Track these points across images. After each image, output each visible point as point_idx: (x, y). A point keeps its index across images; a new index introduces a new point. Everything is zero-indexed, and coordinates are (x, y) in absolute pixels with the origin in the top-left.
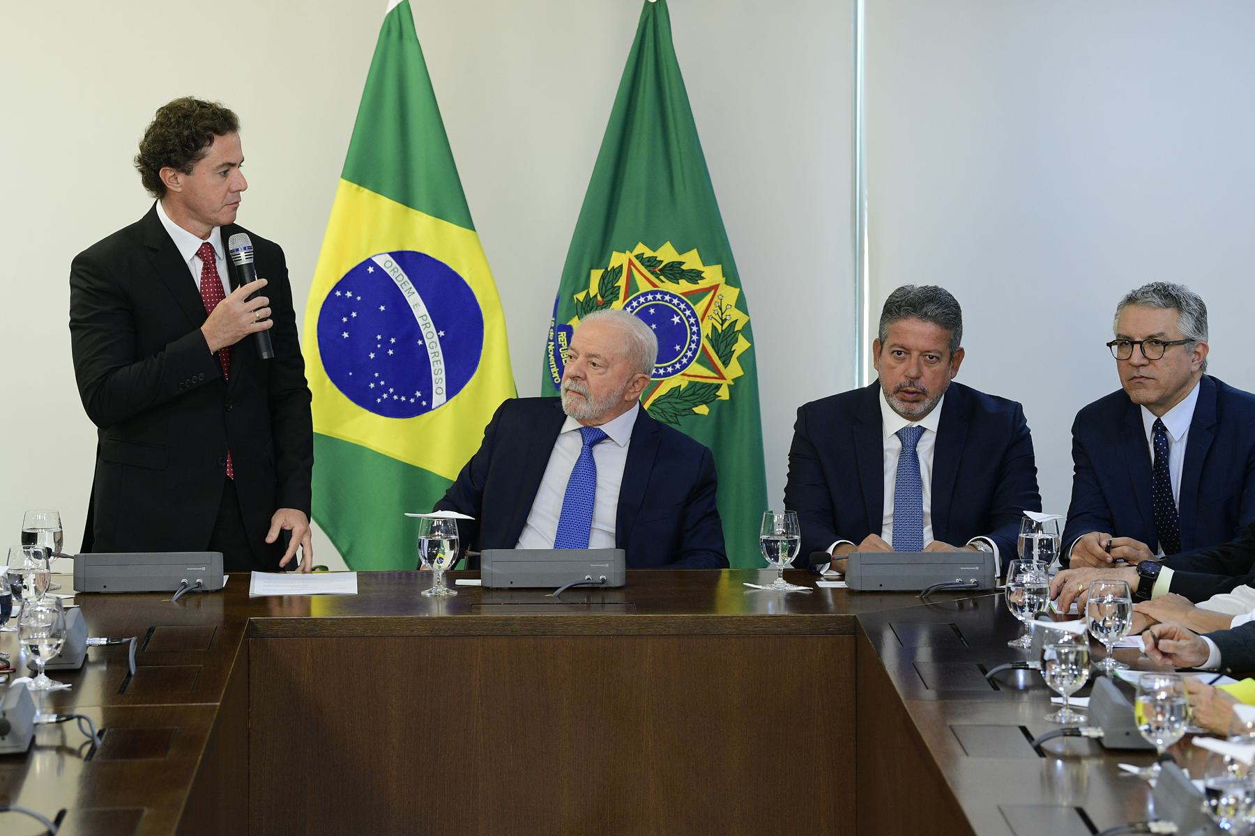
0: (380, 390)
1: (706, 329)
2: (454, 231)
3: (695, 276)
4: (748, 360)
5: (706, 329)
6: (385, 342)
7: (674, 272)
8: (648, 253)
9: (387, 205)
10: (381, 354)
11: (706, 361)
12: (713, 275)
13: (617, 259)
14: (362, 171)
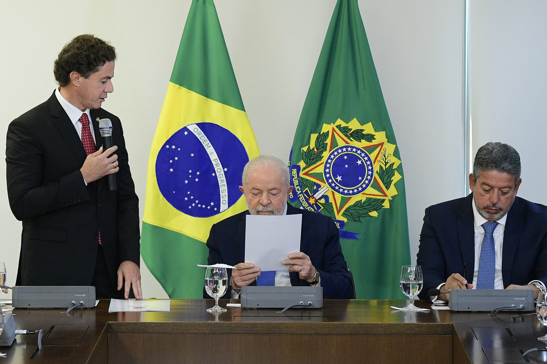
0: (191, 202)
1: (376, 168)
2: (233, 111)
3: (370, 138)
4: (401, 186)
5: (376, 168)
6: (194, 174)
7: (358, 135)
8: (344, 124)
9: (195, 97)
10: (192, 181)
11: (376, 186)
12: (380, 137)
13: (326, 128)
14: (181, 77)
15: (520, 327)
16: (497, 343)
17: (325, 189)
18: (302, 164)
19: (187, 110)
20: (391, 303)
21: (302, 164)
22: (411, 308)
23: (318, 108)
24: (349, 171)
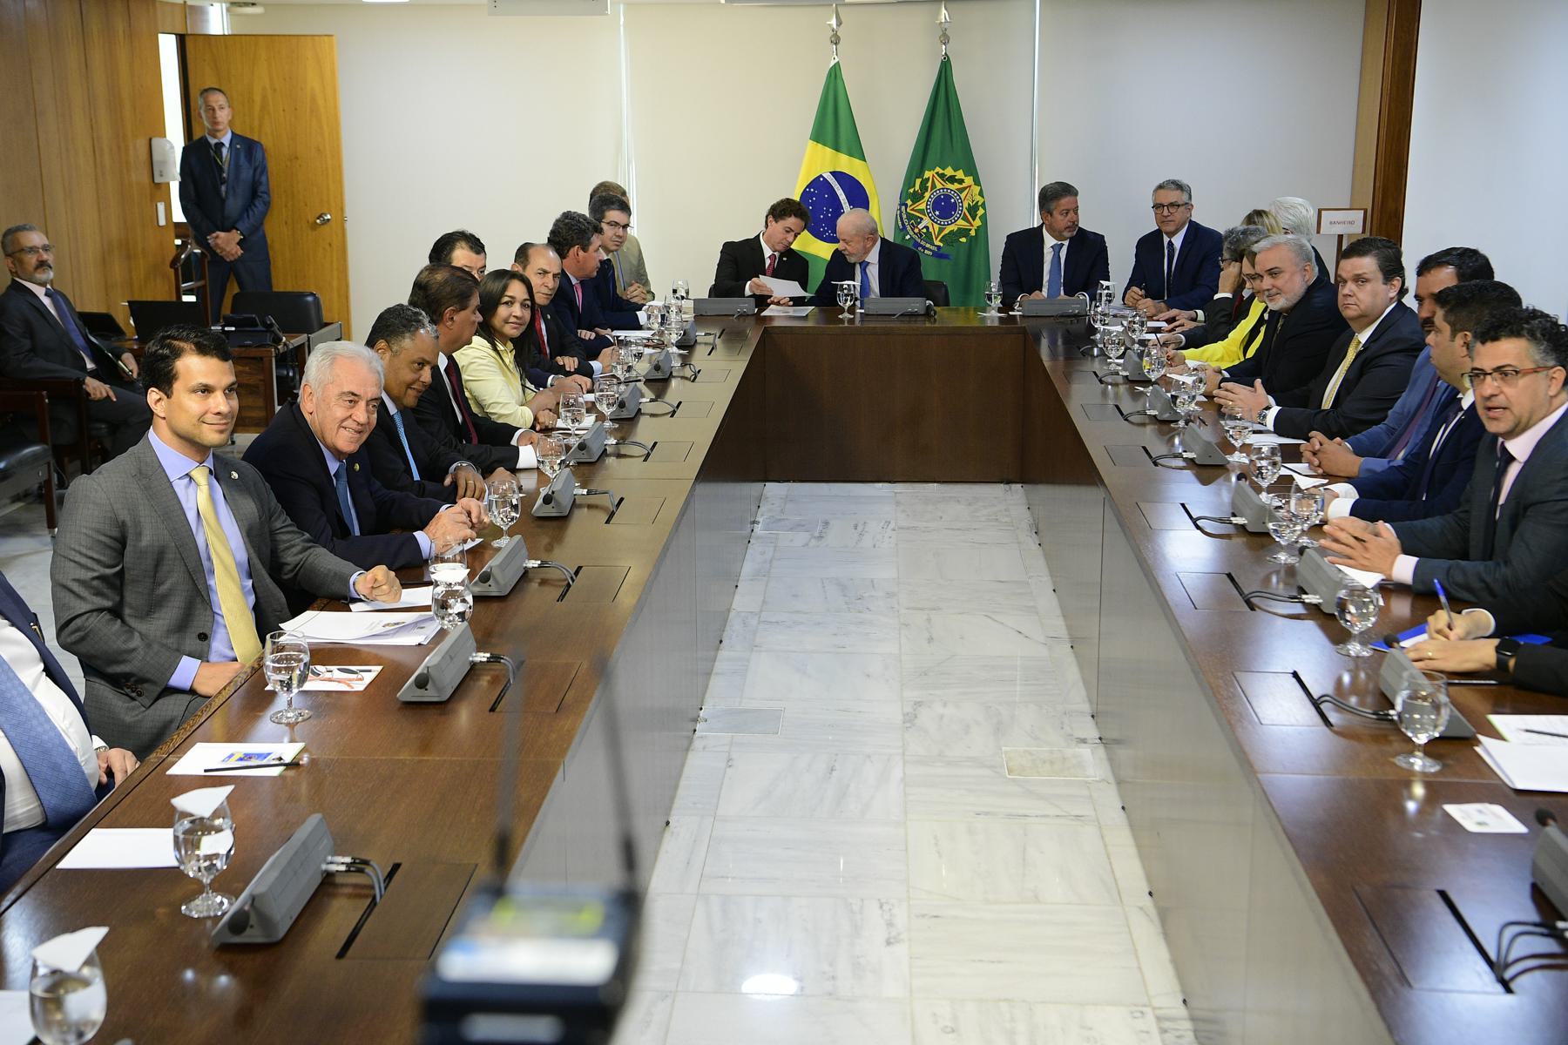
2: (857, 162)
3: (961, 181)
4: (984, 218)
7: (952, 179)
9: (829, 150)
12: (969, 180)
13: (927, 174)
14: (818, 136)
15: (1077, 327)
16: (1060, 342)
17: (926, 221)
18: (909, 202)
19: (821, 162)
20: (976, 310)
21: (909, 202)
22: (994, 314)
23: (922, 159)
24: (945, 207)
